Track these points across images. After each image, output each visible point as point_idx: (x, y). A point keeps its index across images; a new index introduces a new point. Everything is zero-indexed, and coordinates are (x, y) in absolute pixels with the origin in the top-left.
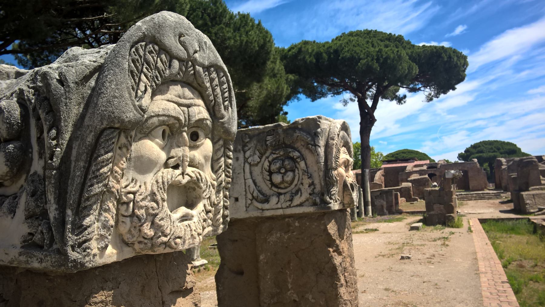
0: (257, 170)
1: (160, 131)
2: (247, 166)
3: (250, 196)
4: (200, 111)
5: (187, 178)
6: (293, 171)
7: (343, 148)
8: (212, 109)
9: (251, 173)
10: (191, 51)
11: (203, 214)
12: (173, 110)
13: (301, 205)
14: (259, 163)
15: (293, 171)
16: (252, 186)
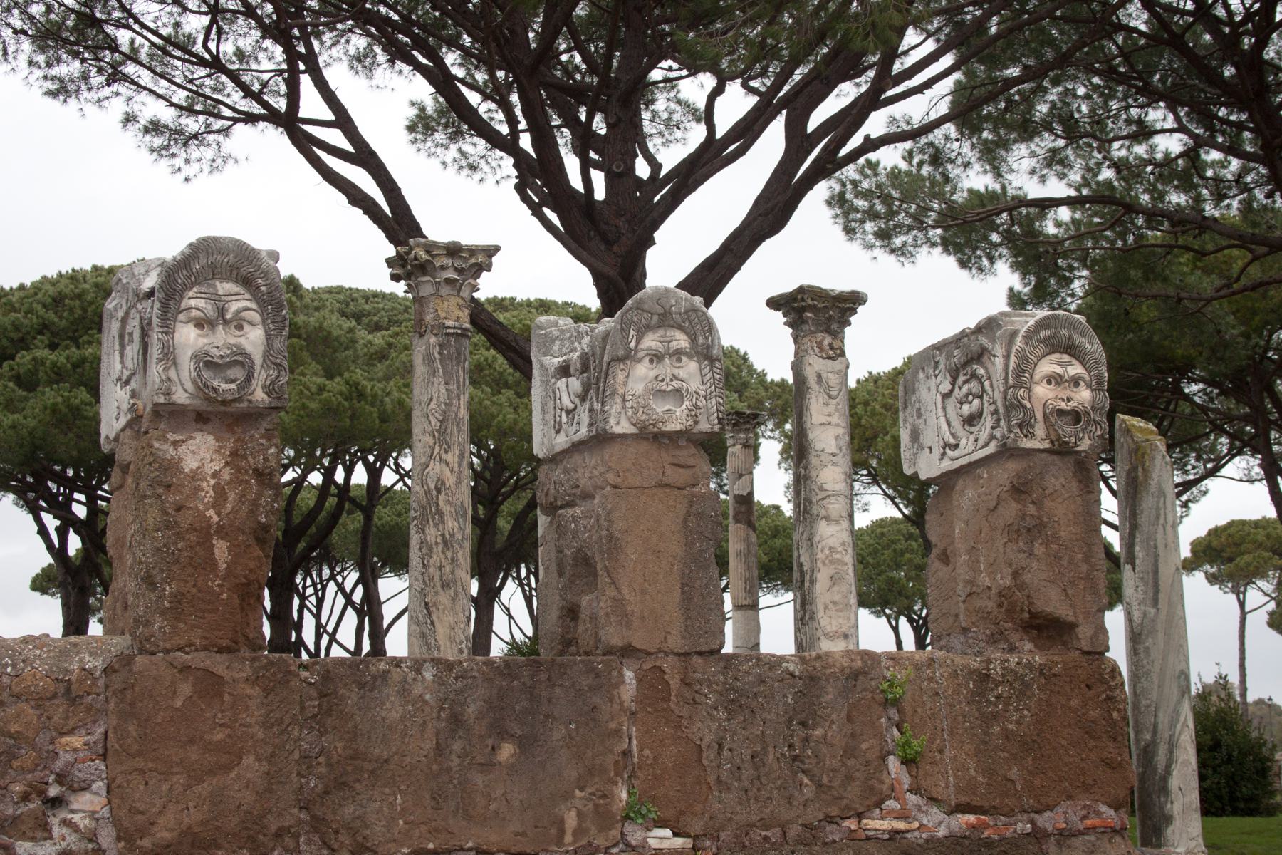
0: (951, 402)
1: (647, 359)
2: (939, 398)
3: (942, 443)
4: (681, 341)
5: (670, 388)
6: (981, 397)
7: (1056, 356)
8: (693, 340)
9: (944, 408)
10: (667, 308)
11: (686, 412)
12: (654, 345)
13: (986, 445)
14: (952, 391)
15: (981, 397)
16: (945, 427)
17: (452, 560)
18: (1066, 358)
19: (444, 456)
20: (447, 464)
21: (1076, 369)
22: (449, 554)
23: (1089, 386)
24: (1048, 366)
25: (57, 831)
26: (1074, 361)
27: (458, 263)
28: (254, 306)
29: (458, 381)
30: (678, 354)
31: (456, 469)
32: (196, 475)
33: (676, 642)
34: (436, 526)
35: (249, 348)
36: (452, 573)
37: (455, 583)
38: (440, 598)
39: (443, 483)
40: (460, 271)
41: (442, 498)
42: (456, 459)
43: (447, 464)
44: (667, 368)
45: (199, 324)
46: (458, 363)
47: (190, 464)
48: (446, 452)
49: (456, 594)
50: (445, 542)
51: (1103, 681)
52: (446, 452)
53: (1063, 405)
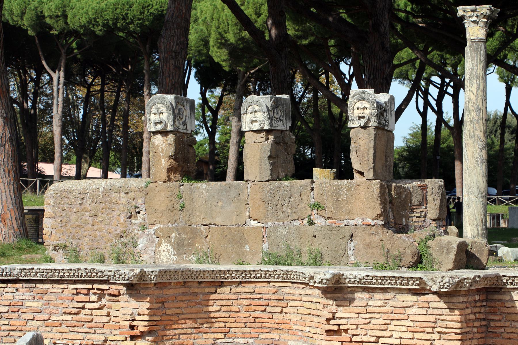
7: (361, 102)
17: (473, 127)
18: (364, 102)
19: (471, 89)
20: (472, 92)
21: (367, 105)
22: (472, 125)
23: (370, 109)
24: (358, 105)
25: (139, 218)
26: (366, 103)
27: (475, 14)
28: (165, 109)
29: (477, 60)
30: (255, 112)
31: (475, 93)
32: (158, 145)
33: (258, 179)
34: (468, 115)
35: (164, 118)
36: (473, 132)
37: (474, 136)
38: (469, 142)
39: (470, 99)
40: (477, 17)
41: (470, 104)
42: (475, 89)
43: (472, 92)
44: (253, 115)
45: (155, 114)
46: (477, 52)
47: (157, 143)
48: (471, 87)
49: (475, 140)
50: (471, 121)
51: (371, 187)
52: (471, 87)
53: (361, 115)
